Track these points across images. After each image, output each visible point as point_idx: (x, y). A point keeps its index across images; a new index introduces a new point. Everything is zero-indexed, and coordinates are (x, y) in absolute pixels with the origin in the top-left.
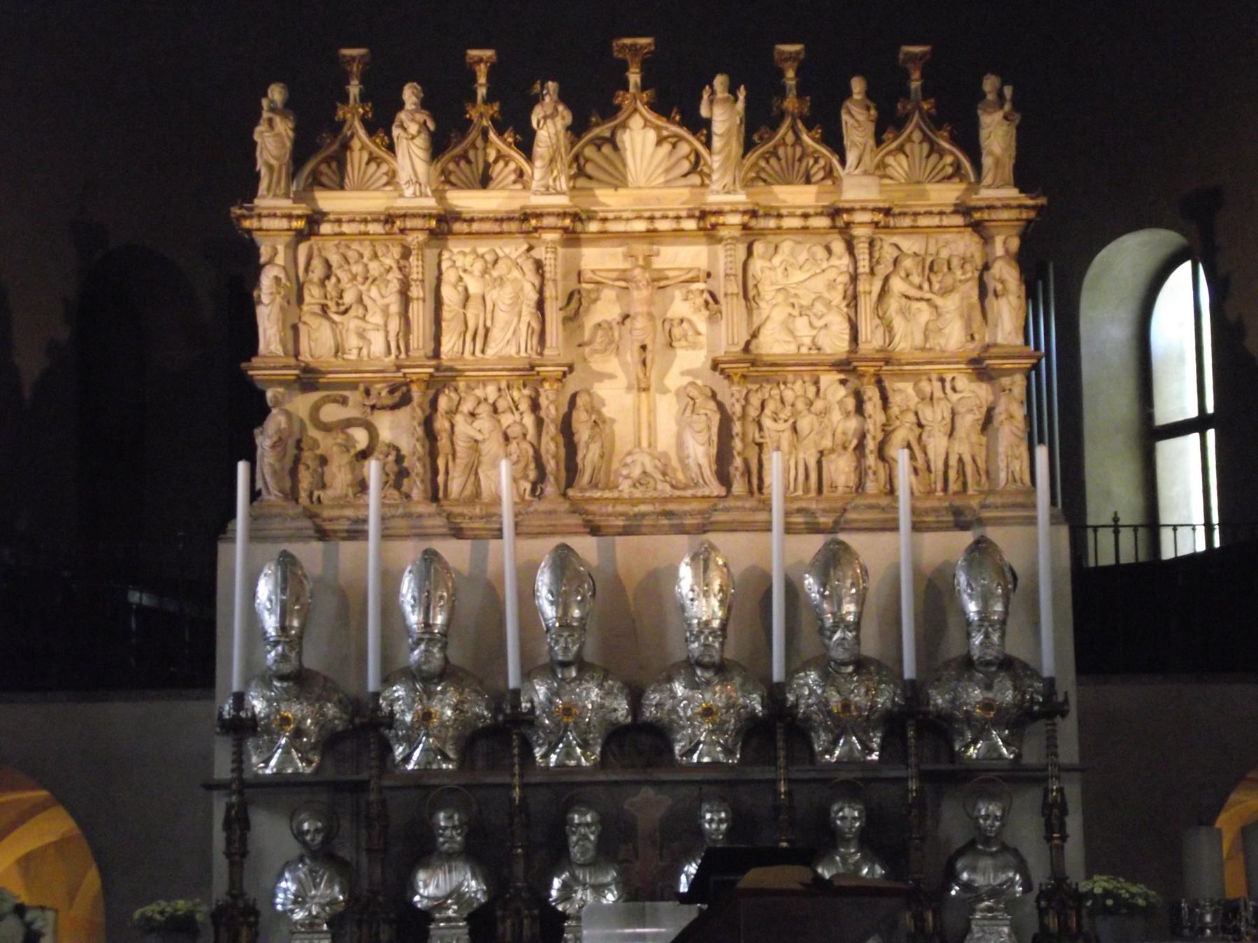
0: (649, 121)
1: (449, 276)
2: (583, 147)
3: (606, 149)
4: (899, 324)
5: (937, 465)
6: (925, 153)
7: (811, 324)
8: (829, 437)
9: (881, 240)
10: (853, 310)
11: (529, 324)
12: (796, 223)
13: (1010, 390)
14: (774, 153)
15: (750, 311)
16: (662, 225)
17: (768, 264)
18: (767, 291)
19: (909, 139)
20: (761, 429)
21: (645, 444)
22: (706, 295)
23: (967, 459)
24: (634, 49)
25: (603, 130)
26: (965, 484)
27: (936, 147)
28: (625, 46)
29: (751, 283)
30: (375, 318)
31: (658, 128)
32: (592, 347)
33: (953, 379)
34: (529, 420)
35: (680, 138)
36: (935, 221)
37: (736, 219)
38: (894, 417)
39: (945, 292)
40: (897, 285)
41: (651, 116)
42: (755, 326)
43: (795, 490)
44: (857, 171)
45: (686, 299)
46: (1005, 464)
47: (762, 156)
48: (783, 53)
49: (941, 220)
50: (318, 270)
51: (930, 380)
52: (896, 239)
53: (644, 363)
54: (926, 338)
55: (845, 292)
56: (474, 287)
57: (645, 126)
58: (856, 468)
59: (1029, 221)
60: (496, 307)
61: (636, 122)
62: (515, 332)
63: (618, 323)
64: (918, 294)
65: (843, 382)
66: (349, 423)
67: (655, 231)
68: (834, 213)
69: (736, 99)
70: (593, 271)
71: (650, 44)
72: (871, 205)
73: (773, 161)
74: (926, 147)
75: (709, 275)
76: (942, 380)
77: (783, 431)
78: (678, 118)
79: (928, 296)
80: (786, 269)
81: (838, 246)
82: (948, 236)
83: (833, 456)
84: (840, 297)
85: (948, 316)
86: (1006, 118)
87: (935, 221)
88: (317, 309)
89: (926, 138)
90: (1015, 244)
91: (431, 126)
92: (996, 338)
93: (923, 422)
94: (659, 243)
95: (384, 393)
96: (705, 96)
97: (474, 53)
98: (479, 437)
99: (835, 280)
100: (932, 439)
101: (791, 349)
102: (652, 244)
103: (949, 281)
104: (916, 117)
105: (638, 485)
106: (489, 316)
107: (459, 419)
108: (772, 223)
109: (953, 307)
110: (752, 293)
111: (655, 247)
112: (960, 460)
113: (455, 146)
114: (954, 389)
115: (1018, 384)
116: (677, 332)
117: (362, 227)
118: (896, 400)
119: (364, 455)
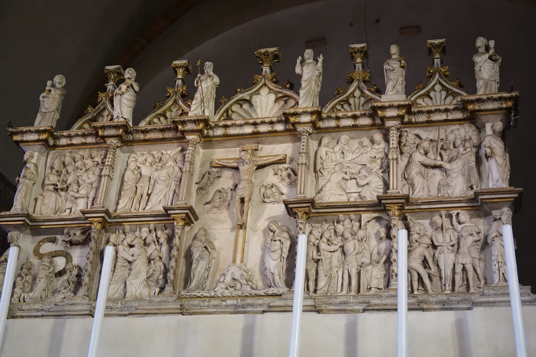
0: (272, 90)
1: (132, 166)
2: (231, 105)
3: (246, 106)
4: (418, 181)
5: (447, 272)
6: (443, 97)
7: (357, 183)
8: (368, 256)
9: (407, 132)
10: (387, 174)
11: (175, 190)
12: (349, 122)
13: (500, 219)
14: (347, 101)
15: (317, 178)
16: (263, 129)
17: (331, 150)
18: (329, 165)
19: (433, 89)
20: (318, 250)
21: (238, 261)
22: (289, 171)
23: (469, 267)
24: (266, 54)
25: (245, 95)
26: (468, 287)
27: (450, 92)
28: (260, 54)
29: (319, 161)
30: (83, 192)
31: (276, 93)
32: (213, 204)
33: (458, 214)
34: (165, 248)
35: (290, 97)
36: (443, 117)
37: (306, 119)
38: (414, 241)
39: (450, 161)
40: (418, 157)
41: (272, 86)
42: (320, 187)
43: (342, 290)
44: (391, 93)
45: (276, 174)
46: (497, 267)
47: (339, 103)
48: (354, 48)
49: (447, 116)
50: (57, 165)
51: (441, 217)
52: (418, 131)
53: (242, 212)
54: (439, 190)
55: (382, 163)
56: (145, 171)
57: (269, 93)
58: (385, 276)
59: (509, 110)
60: (156, 182)
61: (264, 91)
62: (165, 195)
63: (231, 190)
64: (432, 163)
65: (378, 219)
66: (54, 255)
67: (258, 133)
68: (373, 113)
69: (317, 61)
70: (219, 160)
71: (275, 51)
72: (396, 104)
73: (346, 106)
74: (444, 93)
75: (292, 160)
76: (450, 216)
77: (334, 252)
78: (288, 86)
79: (439, 163)
80: (343, 153)
81: (378, 136)
82: (454, 127)
83: (369, 268)
84: (379, 167)
85: (454, 175)
86: (490, 58)
87: (443, 117)
88: (51, 188)
89: (444, 88)
90: (499, 126)
91: (137, 88)
92: (488, 186)
93: (436, 244)
94: (263, 143)
95: (78, 233)
96: (298, 62)
97: (176, 62)
98: (131, 259)
99: (375, 157)
100: (442, 255)
101: (344, 199)
102: (258, 143)
103: (454, 153)
104: (437, 76)
105: (229, 287)
106: (151, 187)
107: (120, 248)
108: (332, 123)
109: (457, 170)
110: (319, 167)
111: (260, 146)
112: (464, 269)
113: (158, 109)
114: (460, 223)
115: (506, 213)
116: (269, 192)
117: (83, 140)
118: (415, 229)
119: (60, 274)
